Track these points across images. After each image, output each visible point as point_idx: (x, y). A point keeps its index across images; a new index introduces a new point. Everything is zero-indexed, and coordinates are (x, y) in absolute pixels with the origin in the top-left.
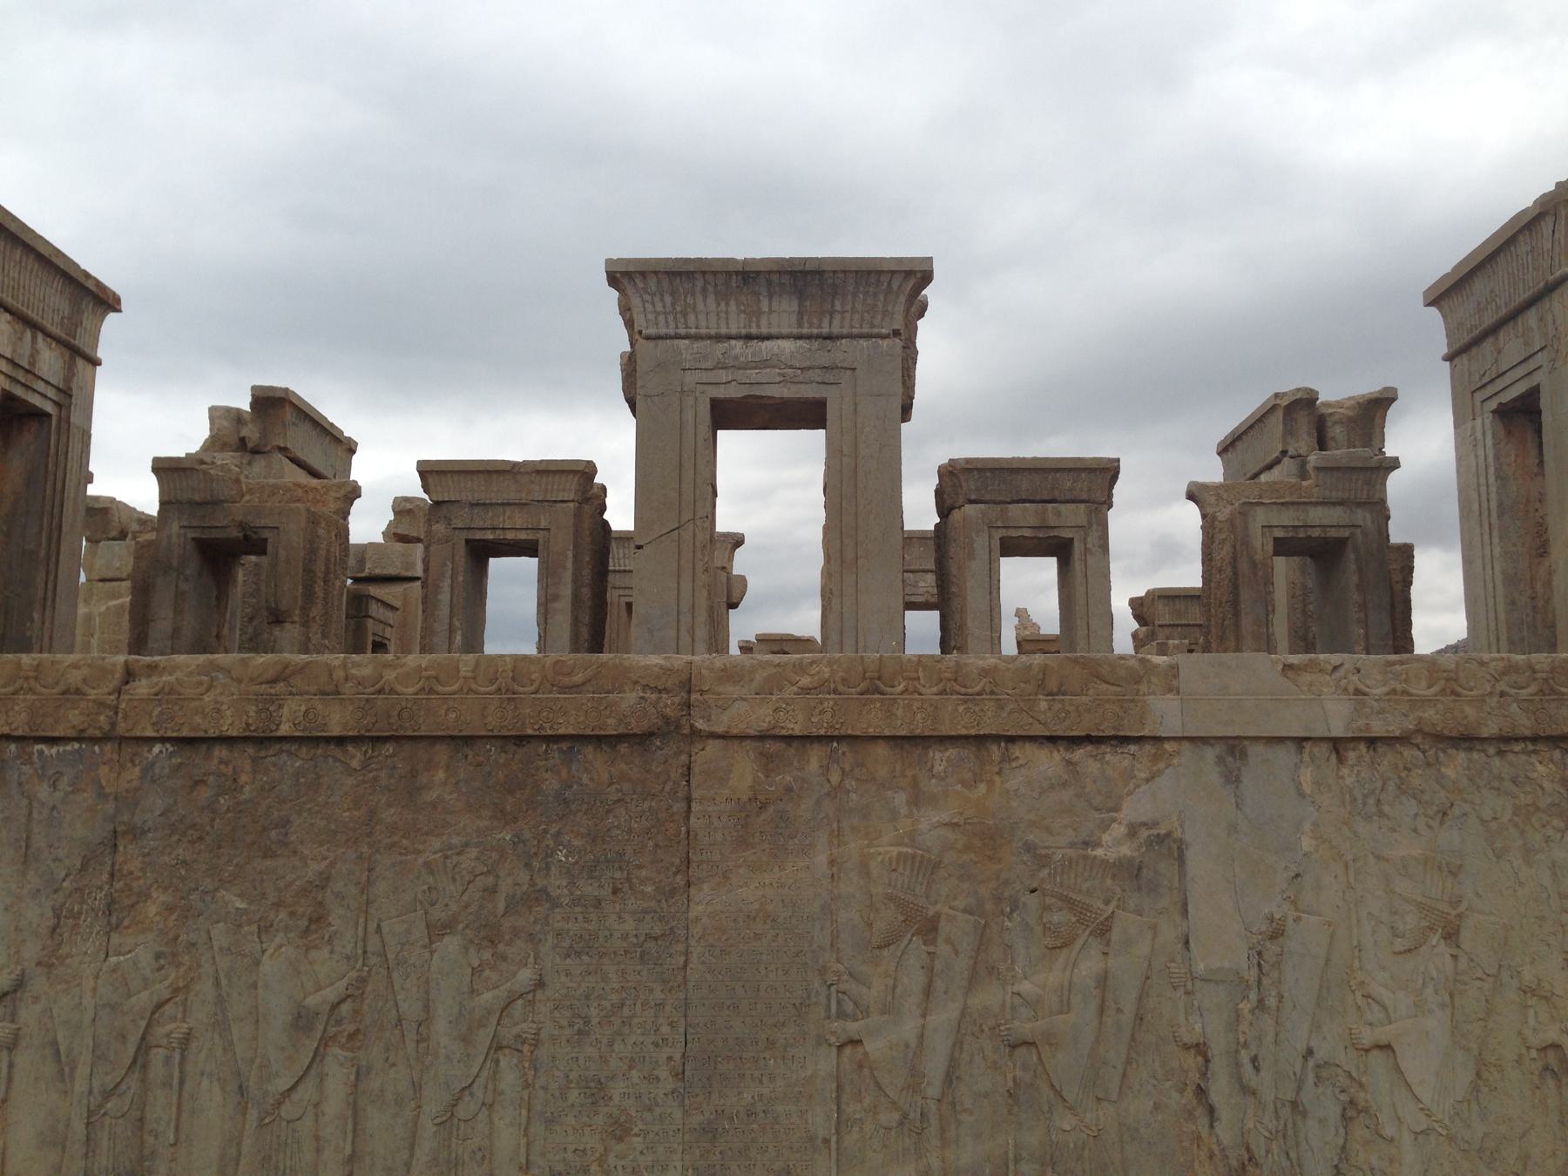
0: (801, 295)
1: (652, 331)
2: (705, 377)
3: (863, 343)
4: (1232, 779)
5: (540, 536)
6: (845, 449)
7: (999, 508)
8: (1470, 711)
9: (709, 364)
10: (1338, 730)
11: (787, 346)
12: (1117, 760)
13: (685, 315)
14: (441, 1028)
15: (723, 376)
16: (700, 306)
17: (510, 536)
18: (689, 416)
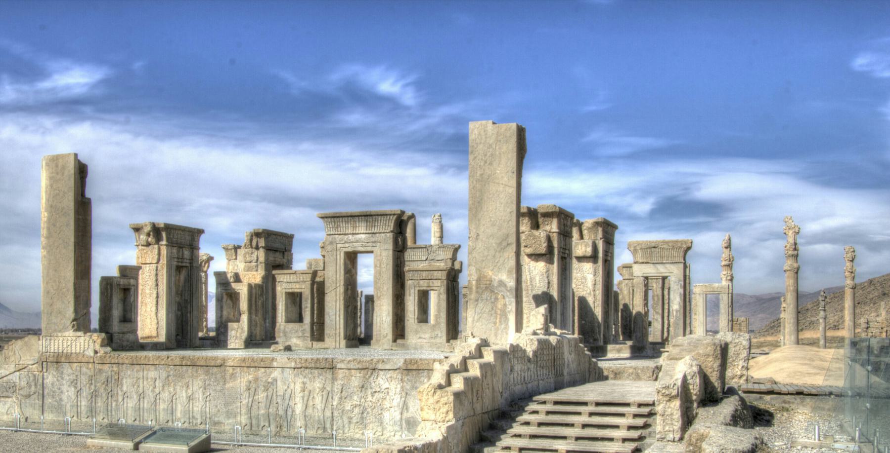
0: (367, 221)
1: (329, 233)
2: (342, 245)
3: (383, 235)
4: (283, 372)
5: (302, 290)
6: (378, 265)
7: (417, 281)
8: (308, 365)
9: (343, 242)
10: (293, 366)
11: (363, 236)
12: (271, 369)
13: (337, 228)
14: (200, 399)
15: (347, 245)
16: (341, 225)
17: (296, 291)
18: (338, 257)
